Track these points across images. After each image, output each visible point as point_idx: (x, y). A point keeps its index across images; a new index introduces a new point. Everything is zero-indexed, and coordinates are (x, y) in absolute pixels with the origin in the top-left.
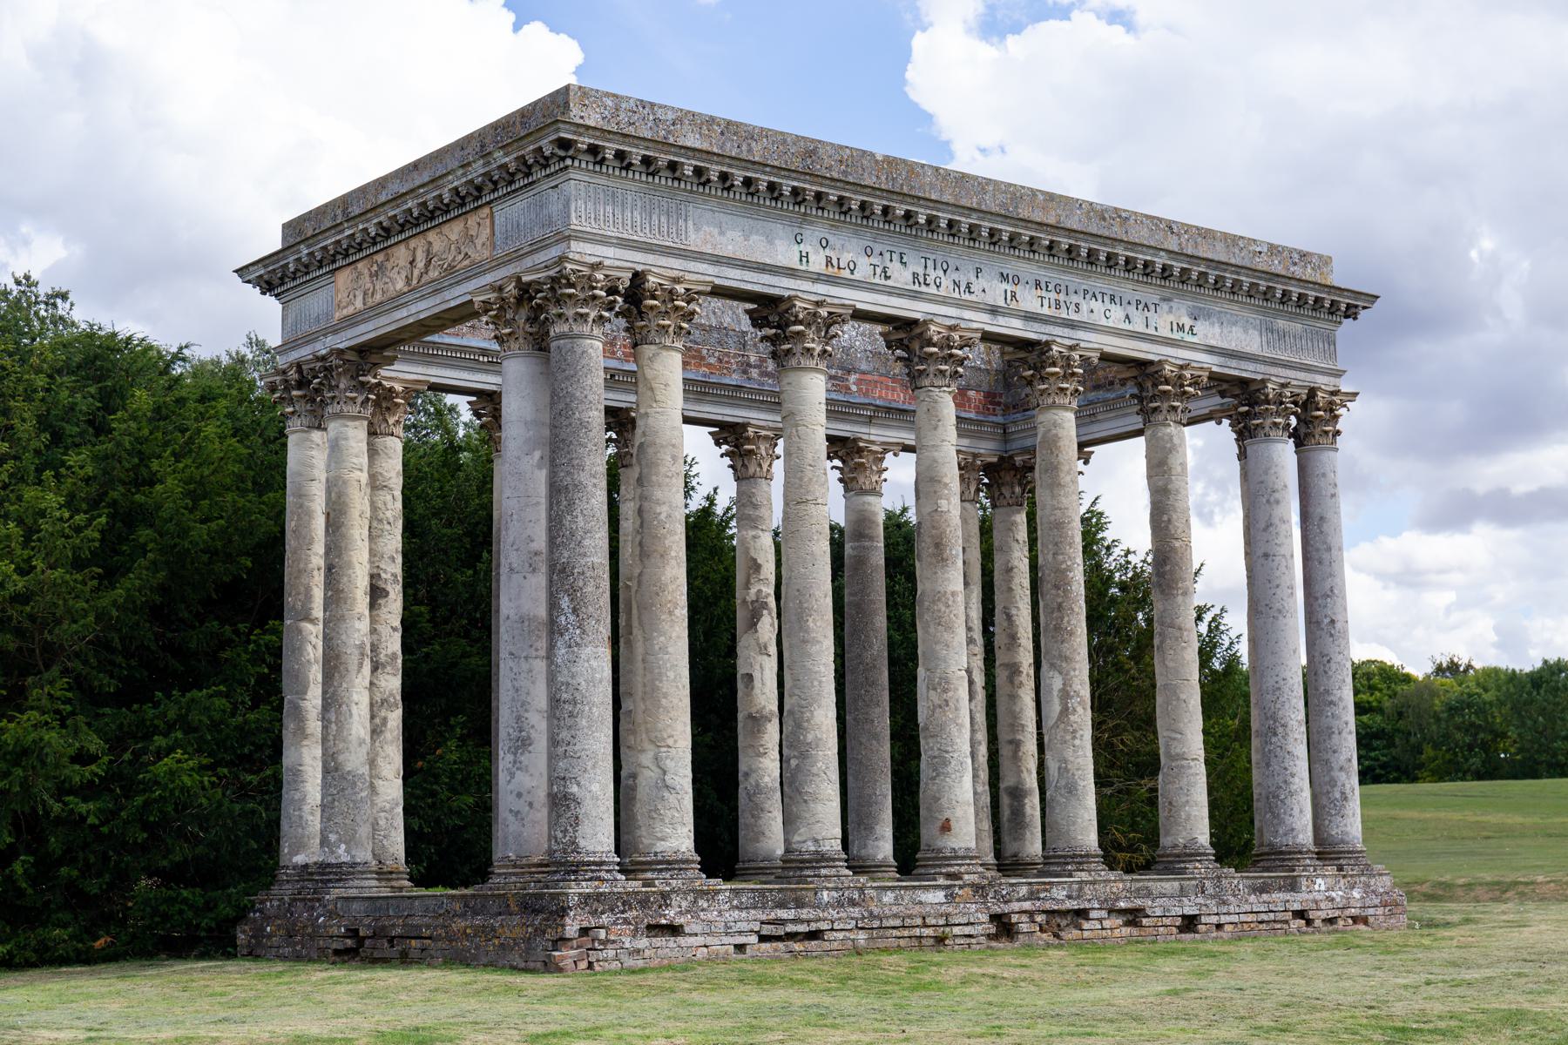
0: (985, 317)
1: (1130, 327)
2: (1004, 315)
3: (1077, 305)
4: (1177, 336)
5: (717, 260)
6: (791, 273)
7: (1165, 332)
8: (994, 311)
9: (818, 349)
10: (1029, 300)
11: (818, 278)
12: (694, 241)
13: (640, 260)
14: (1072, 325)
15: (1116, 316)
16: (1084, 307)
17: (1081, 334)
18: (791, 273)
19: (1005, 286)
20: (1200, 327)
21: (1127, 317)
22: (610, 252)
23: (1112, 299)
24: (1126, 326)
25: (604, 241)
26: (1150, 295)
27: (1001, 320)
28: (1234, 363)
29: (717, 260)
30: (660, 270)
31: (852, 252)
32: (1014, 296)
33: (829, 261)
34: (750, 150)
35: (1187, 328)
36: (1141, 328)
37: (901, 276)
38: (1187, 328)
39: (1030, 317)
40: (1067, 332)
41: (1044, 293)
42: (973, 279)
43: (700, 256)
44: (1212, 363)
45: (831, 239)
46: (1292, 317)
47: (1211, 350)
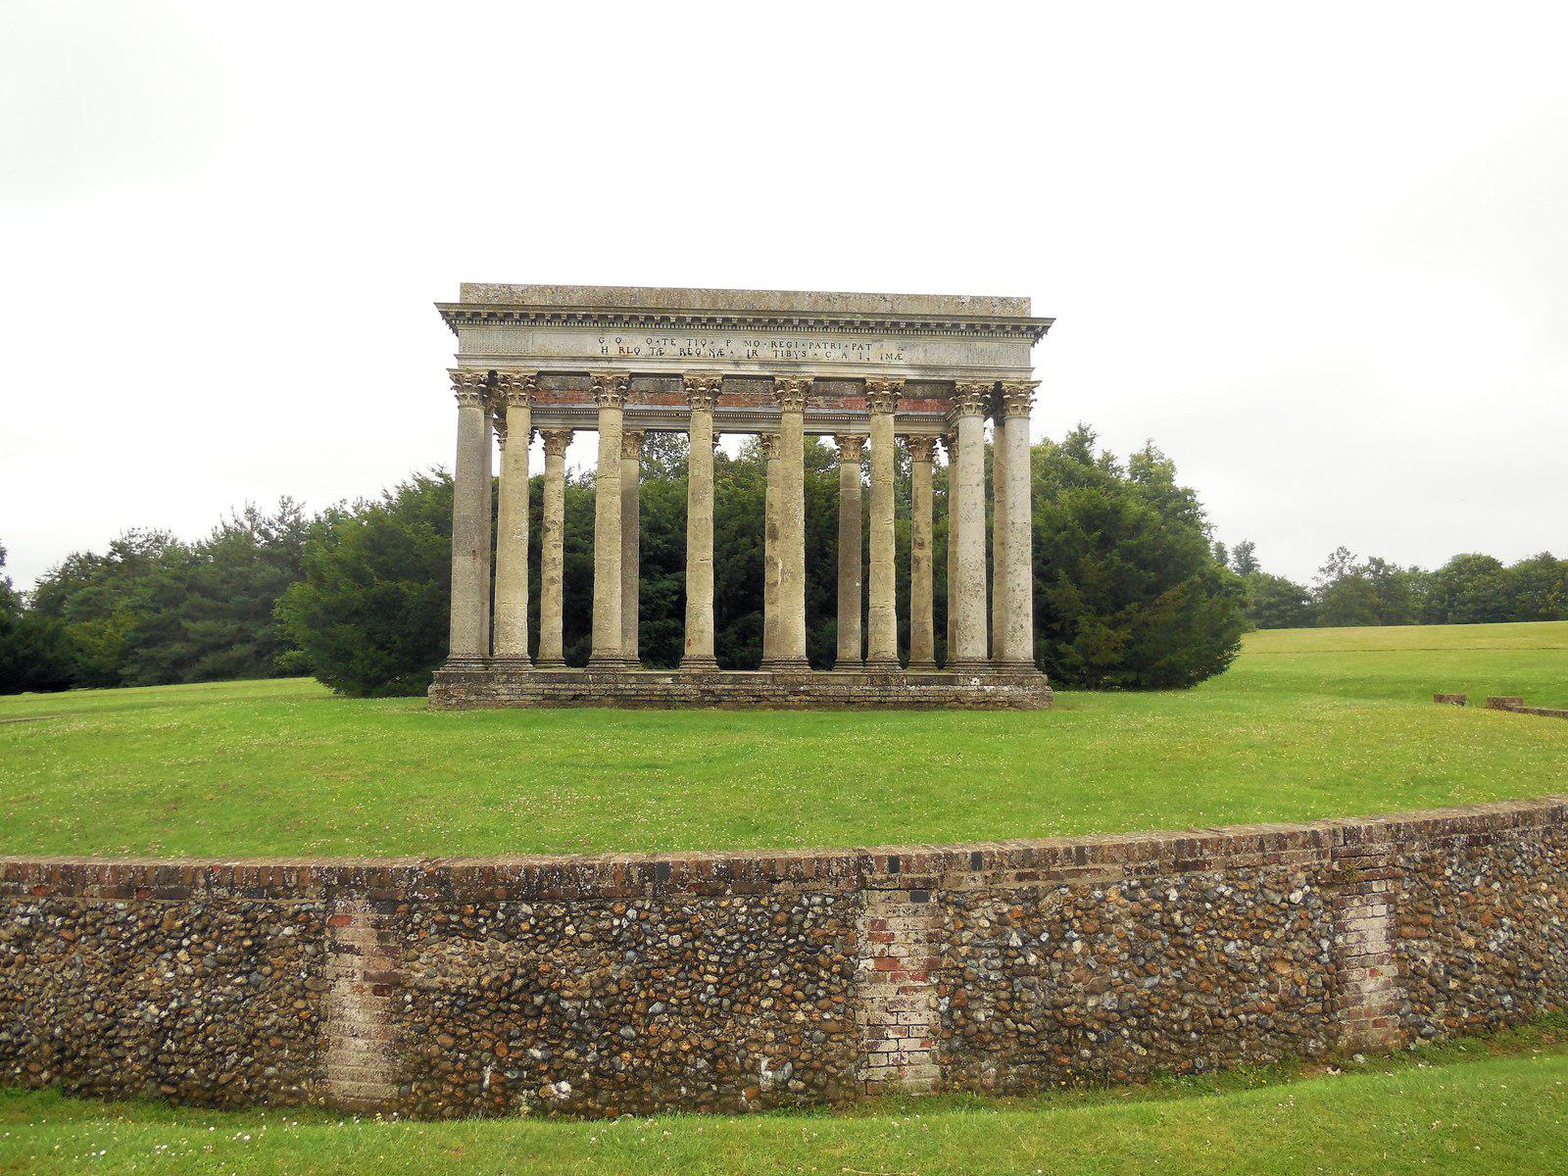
0: (732, 367)
1: (847, 361)
2: (744, 364)
3: (804, 352)
4: (885, 361)
5: (546, 358)
6: (595, 359)
7: (872, 361)
8: (736, 363)
9: (610, 397)
10: (766, 352)
11: (610, 360)
12: (531, 350)
13: (494, 365)
14: (797, 365)
15: (836, 354)
16: (810, 353)
17: (803, 369)
18: (595, 359)
19: (748, 347)
20: (905, 355)
21: (844, 354)
22: (480, 363)
23: (833, 345)
24: (844, 360)
25: (476, 358)
26: (865, 341)
27: (742, 367)
28: (934, 373)
29: (546, 358)
30: (502, 368)
31: (636, 341)
32: (754, 352)
33: (621, 349)
34: (571, 299)
35: (894, 357)
36: (853, 357)
37: (671, 350)
38: (894, 357)
39: (763, 364)
40: (793, 369)
41: (778, 348)
42: (724, 345)
43: (534, 358)
44: (912, 375)
45: (624, 338)
46: (986, 339)
47: (912, 367)
